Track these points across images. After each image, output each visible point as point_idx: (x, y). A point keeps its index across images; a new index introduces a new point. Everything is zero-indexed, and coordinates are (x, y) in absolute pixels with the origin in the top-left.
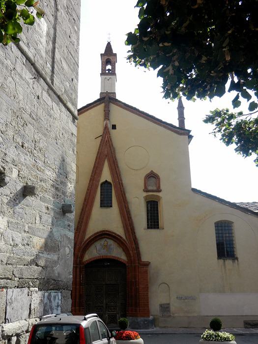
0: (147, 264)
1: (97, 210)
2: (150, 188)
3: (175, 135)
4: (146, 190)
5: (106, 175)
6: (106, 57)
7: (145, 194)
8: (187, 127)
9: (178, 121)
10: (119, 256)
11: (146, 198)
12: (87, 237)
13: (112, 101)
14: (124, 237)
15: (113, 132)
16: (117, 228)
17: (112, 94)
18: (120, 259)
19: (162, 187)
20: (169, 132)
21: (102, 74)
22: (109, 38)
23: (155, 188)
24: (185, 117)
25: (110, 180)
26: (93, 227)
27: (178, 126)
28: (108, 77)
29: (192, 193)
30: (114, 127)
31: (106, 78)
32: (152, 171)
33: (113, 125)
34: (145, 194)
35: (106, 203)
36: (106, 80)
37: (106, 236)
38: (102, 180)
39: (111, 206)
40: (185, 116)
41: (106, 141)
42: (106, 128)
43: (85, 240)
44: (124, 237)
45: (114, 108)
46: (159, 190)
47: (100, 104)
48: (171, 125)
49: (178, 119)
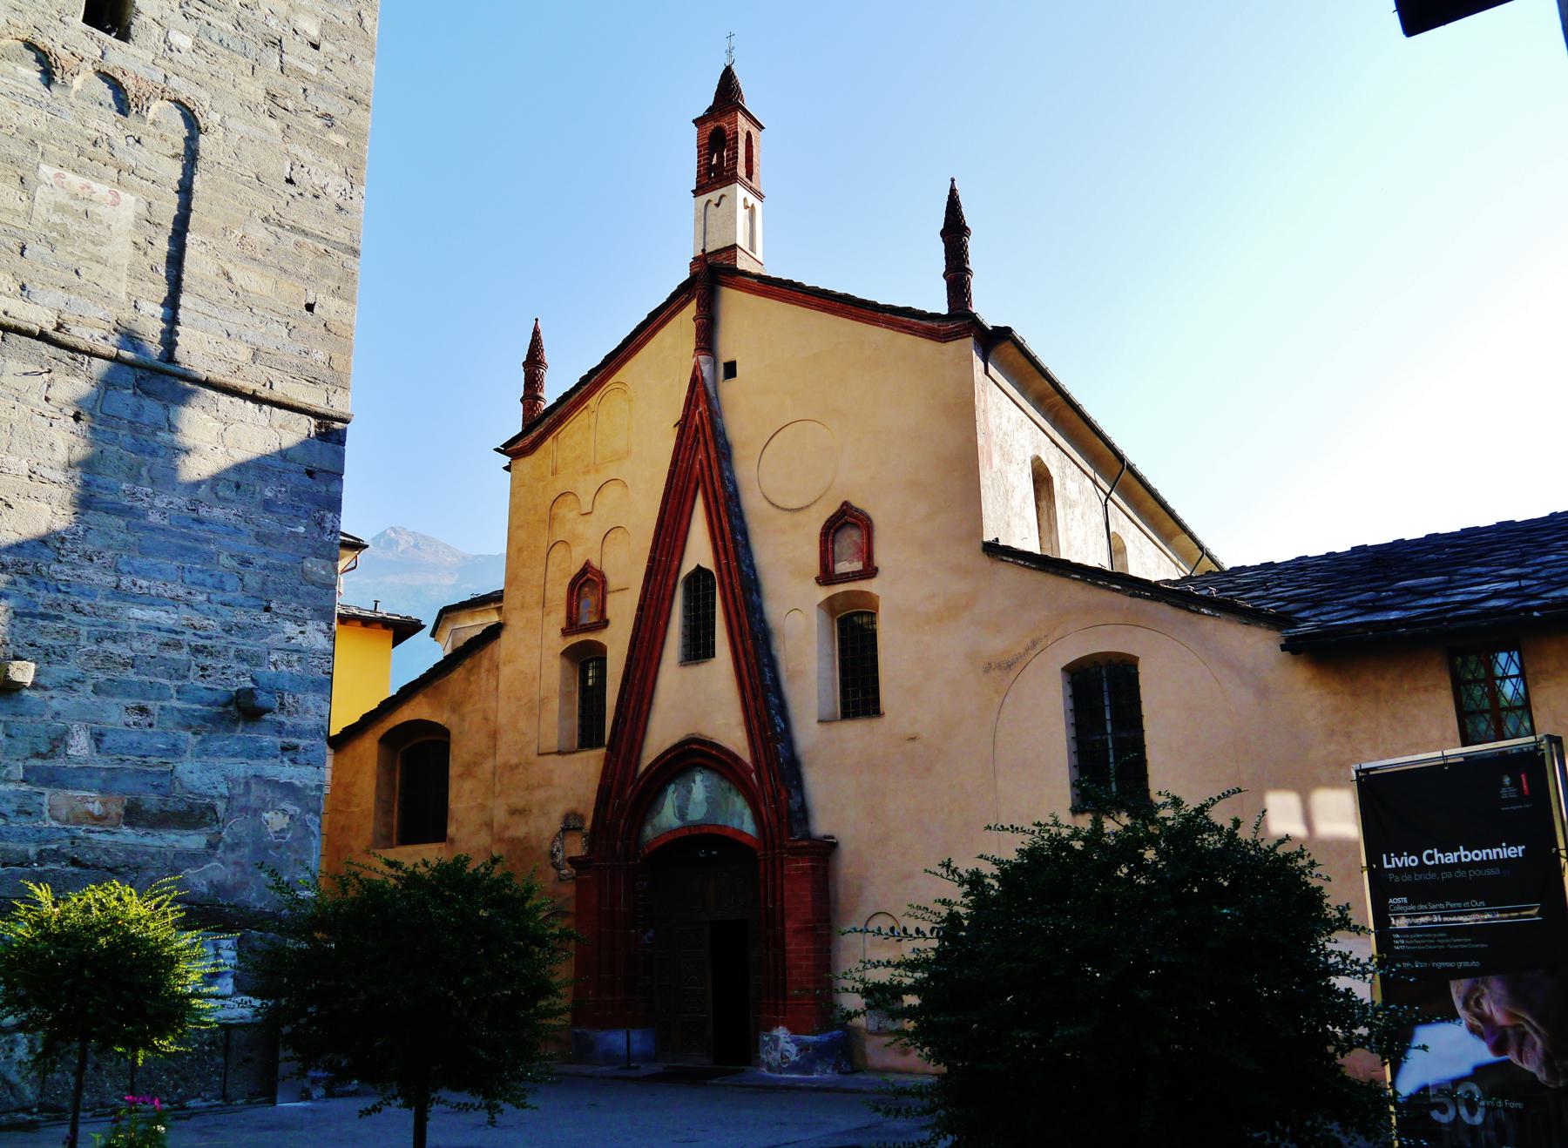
0: (828, 847)
1: (671, 673)
2: (842, 567)
3: (927, 346)
4: (827, 576)
5: (699, 551)
6: (711, 126)
7: (823, 593)
8: (988, 308)
9: (944, 283)
10: (735, 824)
11: (830, 605)
12: (642, 768)
13: (723, 278)
14: (746, 756)
15: (729, 391)
16: (730, 732)
17: (724, 255)
18: (742, 833)
19: (880, 558)
20: (905, 340)
21: (697, 192)
22: (730, 52)
23: (857, 566)
24: (971, 266)
25: (708, 563)
26: (661, 735)
27: (944, 310)
28: (713, 196)
29: (984, 561)
30: (731, 370)
31: (709, 201)
32: (846, 504)
33: (726, 365)
34: (823, 593)
35: (698, 649)
36: (712, 206)
37: (699, 760)
38: (687, 567)
39: (714, 656)
40: (975, 261)
41: (697, 426)
42: (696, 380)
43: (638, 776)
44: (746, 756)
45: (733, 302)
46: (869, 572)
47: (687, 302)
48: (922, 315)
49: (945, 276)
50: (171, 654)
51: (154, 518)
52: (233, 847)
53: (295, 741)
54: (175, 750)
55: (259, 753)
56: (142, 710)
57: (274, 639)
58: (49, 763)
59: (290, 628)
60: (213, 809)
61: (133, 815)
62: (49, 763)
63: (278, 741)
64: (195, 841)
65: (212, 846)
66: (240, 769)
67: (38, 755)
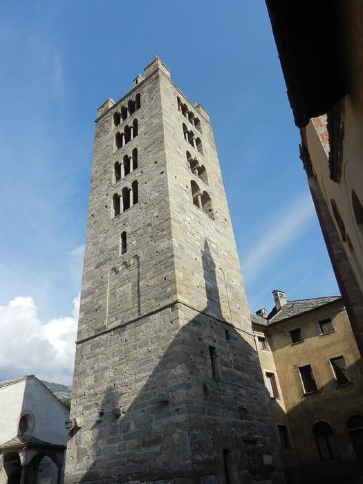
50: (147, 392)
51: (141, 357)
52: (166, 448)
53: (178, 407)
54: (151, 421)
55: (169, 415)
56: (143, 411)
57: (169, 377)
58: (127, 433)
59: (173, 371)
60: (160, 436)
61: (145, 444)
62: (127, 433)
63: (174, 409)
64: (157, 449)
65: (161, 449)
66: (165, 421)
67: (125, 432)
